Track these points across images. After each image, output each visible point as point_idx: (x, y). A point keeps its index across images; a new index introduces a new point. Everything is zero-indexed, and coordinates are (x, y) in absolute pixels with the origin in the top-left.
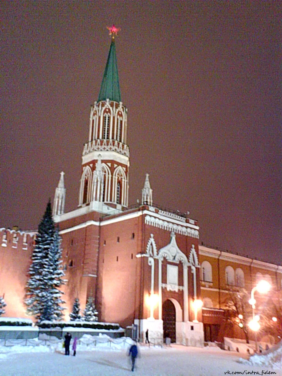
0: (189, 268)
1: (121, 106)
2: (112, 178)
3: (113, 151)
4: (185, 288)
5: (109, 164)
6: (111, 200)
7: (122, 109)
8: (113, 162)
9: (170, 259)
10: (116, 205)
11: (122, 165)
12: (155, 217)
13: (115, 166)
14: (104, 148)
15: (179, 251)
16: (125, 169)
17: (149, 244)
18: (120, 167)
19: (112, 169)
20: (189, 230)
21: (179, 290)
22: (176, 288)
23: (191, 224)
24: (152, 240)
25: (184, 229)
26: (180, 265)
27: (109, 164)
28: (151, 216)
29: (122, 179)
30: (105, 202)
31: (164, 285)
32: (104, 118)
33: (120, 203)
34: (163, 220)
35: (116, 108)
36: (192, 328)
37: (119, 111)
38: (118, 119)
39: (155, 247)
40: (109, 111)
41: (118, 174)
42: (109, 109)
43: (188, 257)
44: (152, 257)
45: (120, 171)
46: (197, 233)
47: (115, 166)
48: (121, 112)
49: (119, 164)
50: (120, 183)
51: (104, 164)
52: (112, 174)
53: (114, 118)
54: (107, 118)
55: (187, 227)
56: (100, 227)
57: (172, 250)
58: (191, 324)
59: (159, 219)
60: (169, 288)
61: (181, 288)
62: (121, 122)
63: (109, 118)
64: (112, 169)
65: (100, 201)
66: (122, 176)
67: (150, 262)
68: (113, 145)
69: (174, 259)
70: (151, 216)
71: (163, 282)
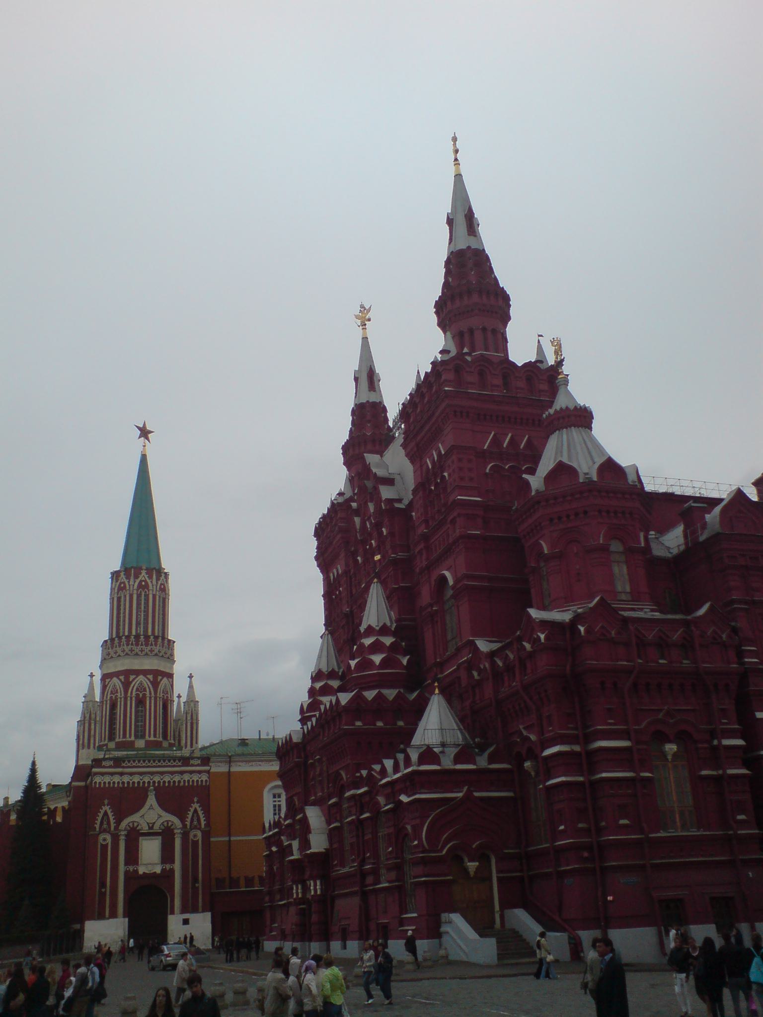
0: (185, 835)
1: (144, 572)
2: (126, 699)
3: (127, 654)
4: (177, 866)
5: (122, 678)
6: (124, 736)
7: (146, 576)
8: (127, 673)
9: (145, 829)
10: (133, 743)
11: (145, 672)
12: (112, 774)
13: (132, 677)
14: (116, 653)
15: (163, 814)
16: (151, 677)
17: (101, 815)
18: (141, 678)
19: (126, 685)
20: (186, 777)
21: (163, 870)
22: (158, 870)
23: (193, 765)
24: (107, 808)
25: (177, 778)
26: (167, 835)
27: (122, 678)
28: (103, 774)
29: (144, 695)
30: (117, 740)
31: (131, 868)
32: (119, 599)
33: (143, 736)
34: (131, 774)
35: (136, 577)
36: (186, 922)
37: (141, 581)
38: (139, 596)
39: (111, 818)
40: (125, 586)
41: (137, 690)
42: (124, 583)
43: (183, 820)
44: (109, 832)
45: (141, 683)
46: (204, 777)
47: (132, 677)
48: (145, 581)
49: (137, 672)
50: (140, 702)
51: (115, 680)
52: (126, 691)
53: (131, 596)
54: (122, 599)
55: (182, 773)
56: (86, 787)
57: (152, 814)
58: (186, 916)
59: (121, 774)
60: (142, 870)
61: (168, 867)
62: (147, 596)
63: (125, 596)
64: (126, 685)
65: (89, 747)
66: (145, 690)
67: (105, 840)
68: (128, 645)
69: (151, 828)
70: (103, 774)
71: (127, 863)
